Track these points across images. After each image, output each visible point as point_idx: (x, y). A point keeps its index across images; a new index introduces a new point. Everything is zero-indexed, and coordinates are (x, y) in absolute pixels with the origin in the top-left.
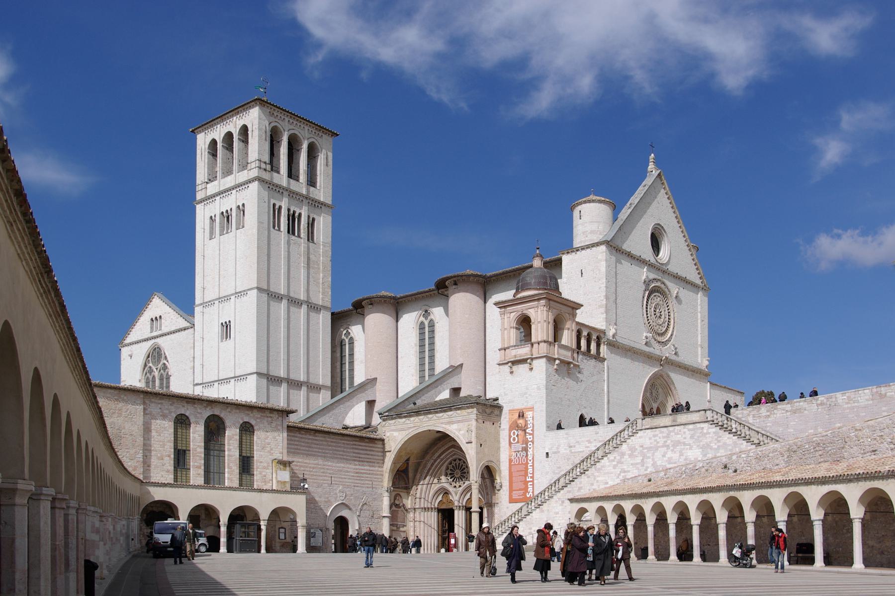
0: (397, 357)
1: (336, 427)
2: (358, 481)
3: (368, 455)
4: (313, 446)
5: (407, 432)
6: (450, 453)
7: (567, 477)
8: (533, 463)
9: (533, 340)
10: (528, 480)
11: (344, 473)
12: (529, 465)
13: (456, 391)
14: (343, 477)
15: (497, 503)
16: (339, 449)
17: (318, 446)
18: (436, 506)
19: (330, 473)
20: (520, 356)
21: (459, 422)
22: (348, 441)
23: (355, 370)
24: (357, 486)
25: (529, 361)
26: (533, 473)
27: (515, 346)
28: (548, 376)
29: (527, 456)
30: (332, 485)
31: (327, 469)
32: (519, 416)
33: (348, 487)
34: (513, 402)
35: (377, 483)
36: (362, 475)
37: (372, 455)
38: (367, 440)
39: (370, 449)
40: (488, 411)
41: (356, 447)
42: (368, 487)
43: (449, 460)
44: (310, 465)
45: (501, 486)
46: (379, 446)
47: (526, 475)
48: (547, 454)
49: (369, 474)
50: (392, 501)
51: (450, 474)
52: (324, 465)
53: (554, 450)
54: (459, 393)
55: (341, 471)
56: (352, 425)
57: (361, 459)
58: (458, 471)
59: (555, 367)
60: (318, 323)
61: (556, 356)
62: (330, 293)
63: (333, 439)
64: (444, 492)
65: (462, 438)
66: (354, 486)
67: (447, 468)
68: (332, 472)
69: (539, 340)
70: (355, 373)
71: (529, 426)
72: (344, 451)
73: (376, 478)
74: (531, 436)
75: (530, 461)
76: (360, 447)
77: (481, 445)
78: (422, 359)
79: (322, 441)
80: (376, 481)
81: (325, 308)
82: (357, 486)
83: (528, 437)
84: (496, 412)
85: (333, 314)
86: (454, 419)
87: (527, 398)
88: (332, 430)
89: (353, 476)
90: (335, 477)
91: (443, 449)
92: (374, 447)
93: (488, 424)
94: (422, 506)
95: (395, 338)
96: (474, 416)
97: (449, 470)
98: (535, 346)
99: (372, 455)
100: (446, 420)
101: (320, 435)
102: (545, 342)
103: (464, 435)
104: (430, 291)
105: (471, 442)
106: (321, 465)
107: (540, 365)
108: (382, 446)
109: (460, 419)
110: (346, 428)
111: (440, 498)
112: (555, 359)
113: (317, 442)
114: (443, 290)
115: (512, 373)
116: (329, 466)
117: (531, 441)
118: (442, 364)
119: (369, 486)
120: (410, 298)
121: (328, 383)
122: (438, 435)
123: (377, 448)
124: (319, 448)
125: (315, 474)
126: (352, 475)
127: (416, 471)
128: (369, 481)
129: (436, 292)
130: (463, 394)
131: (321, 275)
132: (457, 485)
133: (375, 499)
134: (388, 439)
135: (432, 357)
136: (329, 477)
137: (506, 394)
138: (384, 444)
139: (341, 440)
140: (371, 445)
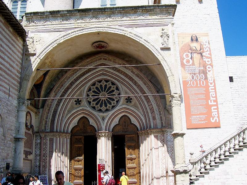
8: (215, 86)
10: (210, 103)
12: (210, 88)
21: (147, 25)
26: (216, 97)
29: (206, 78)
32: (192, 40)
42: (5, 92)
43: (93, 80)
47: (207, 97)
64: (82, 115)
67: (90, 90)
71: (205, 50)
74: (209, 60)
75: (211, 84)
80: (13, 88)
83: (206, 60)
92: (15, 42)
97: (91, 91)
117: (210, 65)
128: (6, 83)
132: (104, 108)
134: (31, 40)
140: (14, 38)
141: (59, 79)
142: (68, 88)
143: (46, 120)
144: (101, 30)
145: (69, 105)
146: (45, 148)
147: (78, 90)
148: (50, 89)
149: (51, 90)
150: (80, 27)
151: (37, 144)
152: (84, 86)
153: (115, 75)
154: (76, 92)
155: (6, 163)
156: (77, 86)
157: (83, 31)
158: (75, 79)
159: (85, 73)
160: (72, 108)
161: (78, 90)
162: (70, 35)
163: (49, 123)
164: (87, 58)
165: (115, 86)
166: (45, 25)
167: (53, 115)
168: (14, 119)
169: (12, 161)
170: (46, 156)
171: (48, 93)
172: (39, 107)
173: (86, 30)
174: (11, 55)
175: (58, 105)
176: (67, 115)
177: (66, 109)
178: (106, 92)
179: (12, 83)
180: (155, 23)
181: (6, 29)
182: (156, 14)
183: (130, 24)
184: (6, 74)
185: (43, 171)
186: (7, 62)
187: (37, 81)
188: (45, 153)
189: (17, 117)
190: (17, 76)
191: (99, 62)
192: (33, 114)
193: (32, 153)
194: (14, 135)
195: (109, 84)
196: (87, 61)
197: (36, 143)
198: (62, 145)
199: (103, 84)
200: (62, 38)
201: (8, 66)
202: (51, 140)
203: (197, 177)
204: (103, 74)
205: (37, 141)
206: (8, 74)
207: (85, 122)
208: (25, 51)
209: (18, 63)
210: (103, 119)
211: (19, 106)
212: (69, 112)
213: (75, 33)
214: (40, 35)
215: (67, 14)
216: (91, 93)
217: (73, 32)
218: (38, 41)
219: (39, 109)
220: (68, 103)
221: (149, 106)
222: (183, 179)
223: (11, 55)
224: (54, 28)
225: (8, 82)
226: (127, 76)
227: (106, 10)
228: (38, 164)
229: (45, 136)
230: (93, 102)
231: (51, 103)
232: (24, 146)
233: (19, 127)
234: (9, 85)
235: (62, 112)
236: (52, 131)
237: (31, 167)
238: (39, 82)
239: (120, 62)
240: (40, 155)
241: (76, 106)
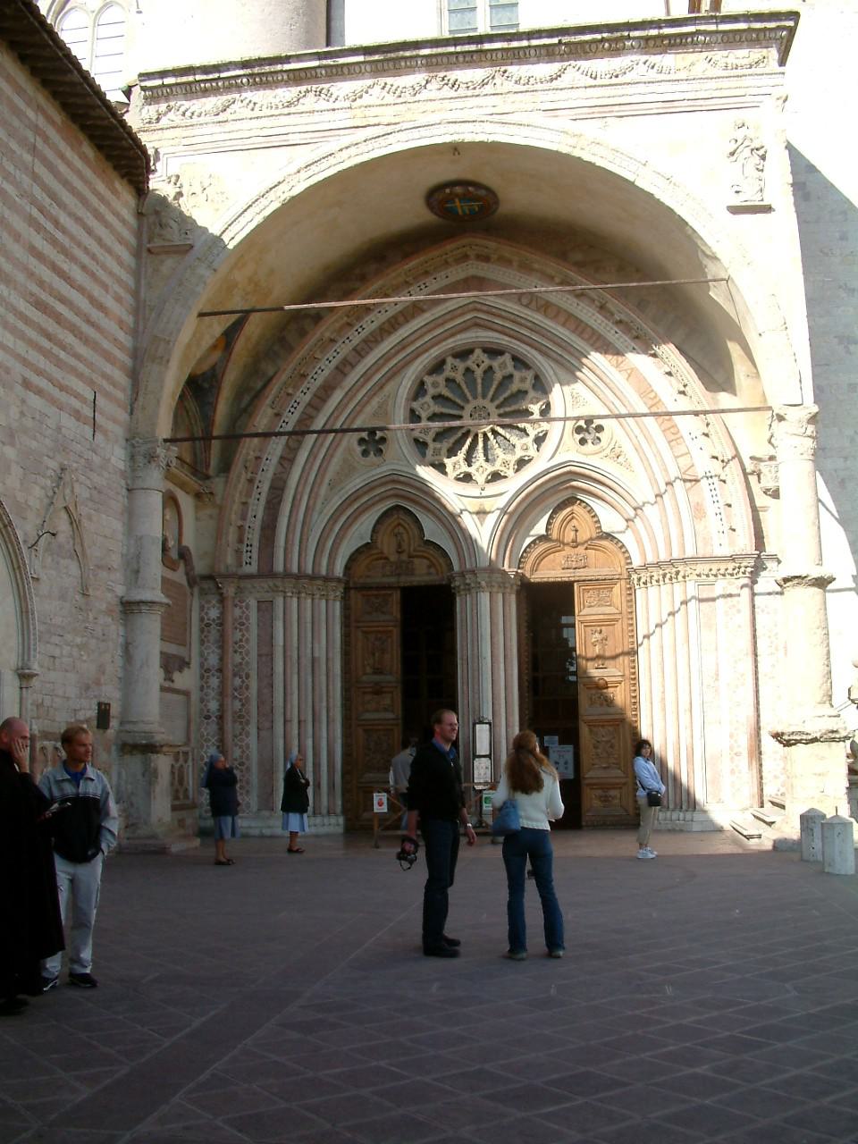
5: (304, 155)
18: (339, 570)
24: (39, 392)
42: (77, 415)
43: (435, 352)
57: (59, 235)
66: (27, 384)
67: (420, 390)
76: (62, 168)
80: (107, 395)
82: (39, 392)
97: (428, 398)
100: (578, 99)
105: (767, 209)
111: (361, 531)
126: (23, 306)
128: (80, 376)
140: (101, 187)
141: (290, 349)
143: (240, 523)
144: (467, 134)
145: (335, 460)
146: (241, 640)
148: (253, 393)
149: (258, 395)
151: (208, 625)
152: (397, 379)
153: (529, 324)
155: (95, 702)
158: (358, 348)
159: (401, 319)
160: (348, 470)
162: (332, 160)
163: (254, 537)
164: (407, 256)
165: (530, 375)
167: (268, 502)
168: (118, 526)
169: (117, 695)
170: (248, 676)
171: (245, 410)
172: (211, 472)
173: (402, 136)
174: (94, 257)
175: (287, 460)
176: (327, 500)
177: (323, 476)
178: (492, 400)
179: (105, 376)
181: (69, 154)
184: (81, 339)
185: (236, 736)
186: (81, 289)
187: (200, 361)
188: (241, 664)
189: (130, 515)
190: (122, 347)
191: (458, 273)
192: (186, 501)
193: (188, 664)
194: (120, 590)
195: (503, 366)
196: (406, 267)
197: (202, 620)
198: (309, 626)
199: (478, 366)
200: (303, 175)
202: (266, 607)
204: (477, 324)
205: (207, 614)
206: (86, 340)
207: (405, 528)
208: (145, 237)
209: (121, 292)
211: (133, 470)
213: (353, 150)
215: (318, 71)
216: (426, 406)
218: (198, 190)
219: (208, 477)
220: (330, 452)
221: (676, 457)
223: (94, 257)
225: (87, 371)
226: (580, 329)
228: (213, 706)
229: (240, 590)
230: (438, 445)
231: (260, 450)
232: (158, 631)
233: (138, 556)
234: (91, 383)
235: (308, 489)
236: (267, 572)
237: (189, 722)
238: (206, 367)
239: (552, 266)
240: (220, 670)
241: (364, 461)
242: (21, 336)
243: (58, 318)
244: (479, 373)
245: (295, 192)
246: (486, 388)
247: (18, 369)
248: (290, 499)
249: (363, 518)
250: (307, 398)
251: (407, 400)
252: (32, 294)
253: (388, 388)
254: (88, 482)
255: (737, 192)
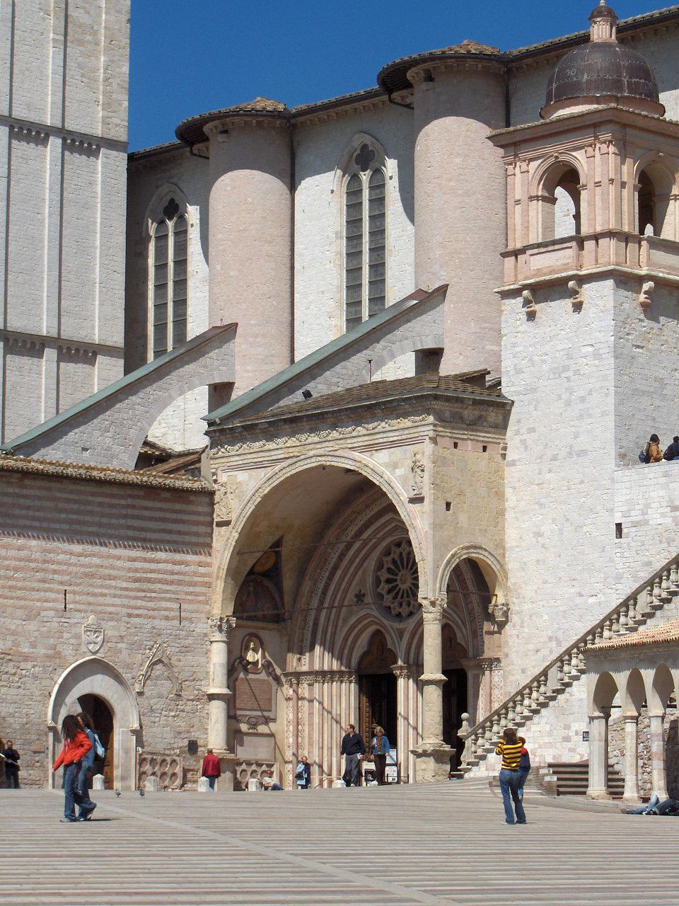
0: (292, 268)
1: (122, 462)
2: (140, 603)
3: (170, 532)
4: (17, 512)
6: (385, 525)
7: (656, 591)
9: (585, 230)
11: (99, 582)
13: (429, 358)
14: (98, 591)
15: (498, 660)
16: (88, 518)
17: (31, 513)
19: (61, 583)
20: (551, 273)
21: (392, 444)
22: (113, 496)
23: (189, 302)
24: (138, 616)
25: (571, 284)
27: (539, 246)
28: (622, 324)
30: (67, 614)
31: (55, 572)
33: (112, 617)
34: (534, 390)
35: (195, 607)
36: (152, 586)
37: (179, 533)
38: (167, 495)
39: (174, 516)
40: (469, 413)
41: (136, 512)
42: (167, 618)
43: (384, 544)
44: (7, 563)
45: (506, 614)
46: (200, 509)
48: (619, 526)
49: (172, 583)
50: (236, 654)
51: (388, 581)
52: (45, 562)
53: (636, 516)
54: (438, 363)
55: (92, 576)
56: (179, 448)
58: (403, 572)
59: (642, 297)
60: (92, 183)
61: (643, 272)
62: (126, 104)
63: (71, 492)
65: (398, 486)
66: (130, 615)
67: (380, 566)
68: (66, 578)
69: (599, 229)
70: (190, 311)
72: (100, 525)
73: (190, 593)
76: (147, 513)
77: (448, 505)
78: (353, 272)
79: (39, 498)
80: (191, 602)
81: (112, 144)
82: (138, 616)
84: (493, 416)
85: (132, 158)
86: (380, 439)
87: (568, 379)
88: (70, 471)
89: (126, 589)
90: (74, 593)
91: (370, 513)
93: (469, 449)
94: (317, 667)
95: (289, 217)
96: (428, 431)
98: (589, 245)
99: (179, 533)
101: (38, 483)
102: (610, 234)
103: (404, 480)
104: (369, 95)
106: (35, 561)
107: (600, 295)
108: (206, 509)
109: (393, 437)
110: (151, 457)
112: (641, 279)
113: (29, 502)
114: (404, 92)
115: (531, 316)
116: (60, 563)
118: (399, 287)
119: (172, 614)
120: (323, 115)
121: (117, 337)
122: (351, 479)
123: (194, 513)
124: (33, 519)
125: (20, 584)
126: (125, 585)
127: (301, 573)
128: (170, 600)
129: (385, 98)
130: (450, 366)
131: (102, 59)
132: (405, 610)
133: (186, 650)
134: (223, 490)
135: (378, 268)
136: (58, 592)
137: (519, 371)
138: (212, 504)
139: (93, 494)
140: (178, 506)
142: (335, 568)
144: (323, 461)
147: (357, 569)
150: (292, 457)
152: (367, 562)
154: (354, 575)
156: (351, 562)
157: (297, 465)
161: (357, 569)
166: (240, 455)
173: (301, 463)
180: (404, 437)
182: (405, 415)
183: (366, 443)
201: (170, 567)
203: (468, 765)
210: (401, 634)
212: (345, 621)
214: (236, 476)
217: (282, 470)
222: (424, 766)
224: (254, 461)
227: (325, 416)
241: (355, 608)
242: (127, 597)
243: (149, 580)
244: (404, 555)
245: (266, 492)
246: (403, 567)
247: (125, 611)
248: (321, 630)
249: (364, 635)
250: (327, 574)
251: (374, 571)
252: (130, 578)
253: (365, 565)
254: (178, 645)
255: (414, 490)
